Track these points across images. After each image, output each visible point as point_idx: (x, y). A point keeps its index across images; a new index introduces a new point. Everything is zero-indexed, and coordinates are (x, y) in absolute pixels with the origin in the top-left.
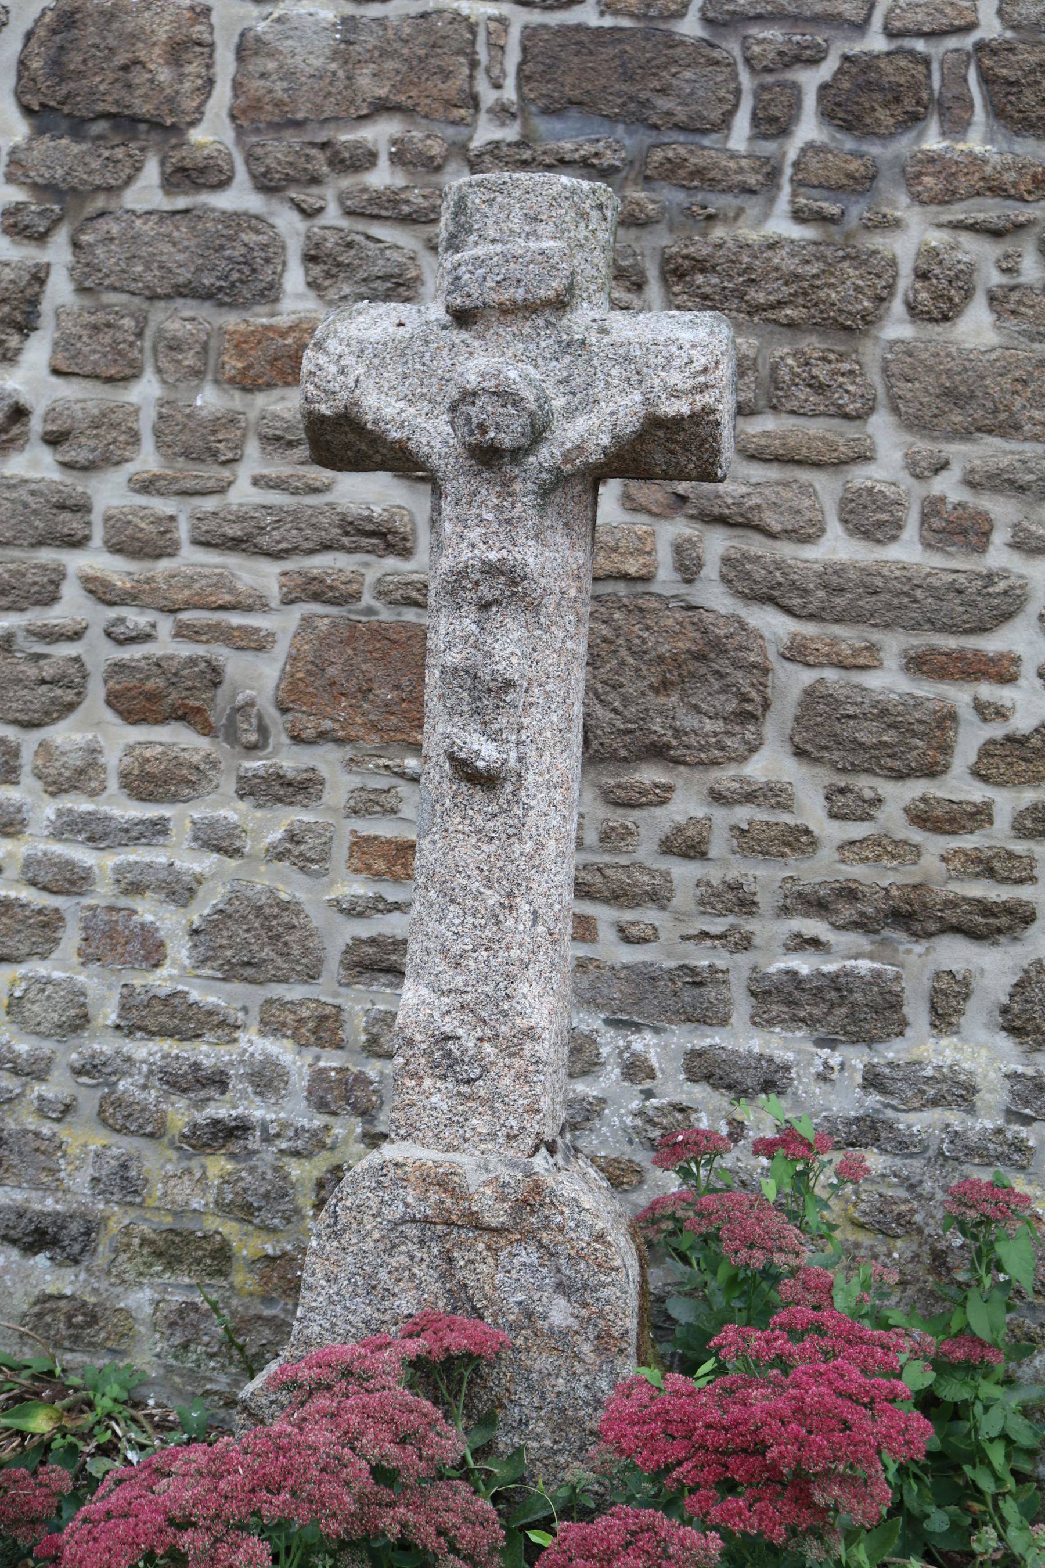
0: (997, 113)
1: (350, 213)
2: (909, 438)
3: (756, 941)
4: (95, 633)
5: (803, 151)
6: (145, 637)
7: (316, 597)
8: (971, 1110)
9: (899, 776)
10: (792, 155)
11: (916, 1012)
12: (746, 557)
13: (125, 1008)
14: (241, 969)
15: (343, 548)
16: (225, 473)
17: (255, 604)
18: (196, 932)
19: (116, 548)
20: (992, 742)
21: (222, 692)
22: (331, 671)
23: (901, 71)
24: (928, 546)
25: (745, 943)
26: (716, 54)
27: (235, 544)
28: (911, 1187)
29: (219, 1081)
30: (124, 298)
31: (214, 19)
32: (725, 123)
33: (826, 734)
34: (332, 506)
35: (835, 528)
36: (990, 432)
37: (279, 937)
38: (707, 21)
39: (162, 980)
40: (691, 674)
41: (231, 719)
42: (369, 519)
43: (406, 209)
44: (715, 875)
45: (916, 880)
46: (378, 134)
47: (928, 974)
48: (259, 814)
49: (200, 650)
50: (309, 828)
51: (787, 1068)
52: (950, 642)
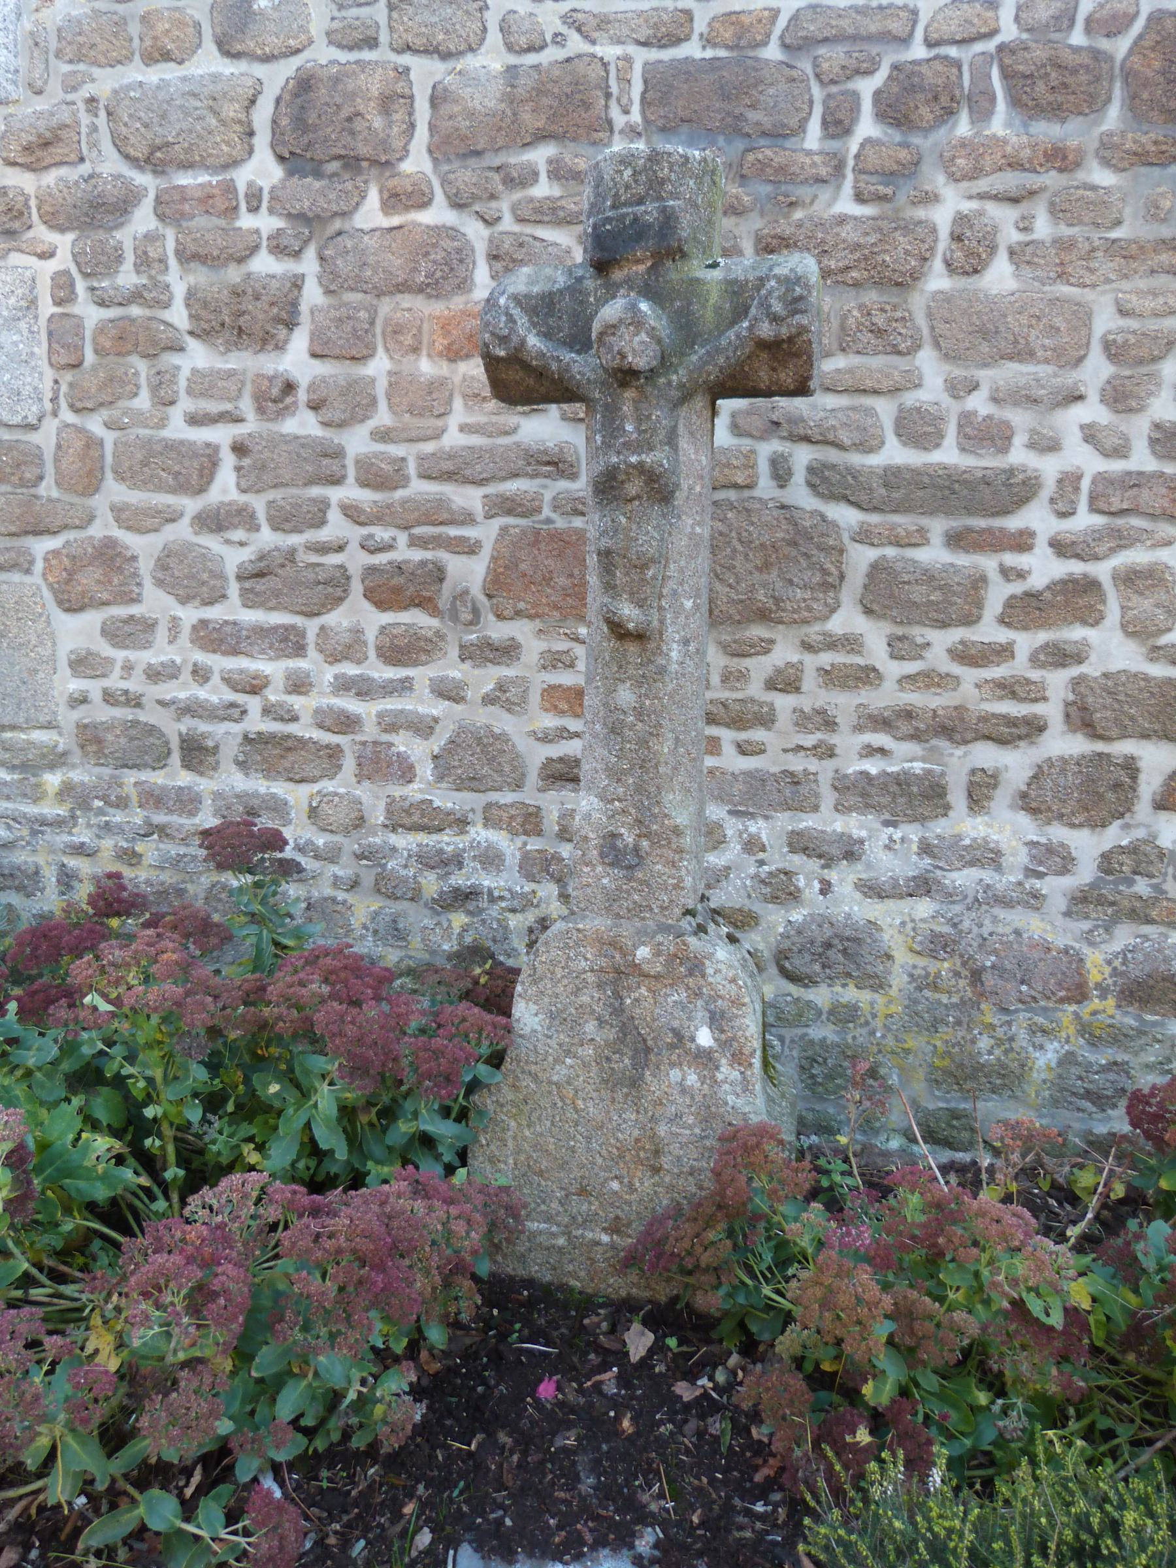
0: (1015, 102)
1: (521, 220)
2: (947, 367)
3: (837, 751)
4: (354, 546)
5: (862, 145)
6: (389, 547)
7: (510, 512)
8: (999, 868)
9: (944, 625)
10: (854, 148)
11: (957, 798)
12: (825, 466)
13: (389, 812)
14: (471, 783)
15: (527, 475)
16: (440, 423)
17: (468, 519)
18: (435, 757)
19: (364, 484)
20: (1013, 597)
21: (446, 587)
22: (523, 566)
23: (937, 74)
24: (963, 450)
25: (831, 753)
26: (794, 73)
27: (449, 476)
28: (955, 925)
29: (457, 861)
30: (360, 296)
31: (413, 76)
32: (802, 127)
33: (885, 593)
34: (518, 445)
35: (891, 440)
36: (1011, 359)
37: (494, 758)
38: (785, 46)
39: (414, 791)
40: (786, 557)
41: (453, 603)
42: (545, 452)
43: (561, 214)
44: (806, 703)
45: (957, 703)
46: (540, 156)
47: (965, 771)
48: (476, 672)
49: (429, 555)
50: (514, 681)
51: (861, 842)
52: (981, 523)
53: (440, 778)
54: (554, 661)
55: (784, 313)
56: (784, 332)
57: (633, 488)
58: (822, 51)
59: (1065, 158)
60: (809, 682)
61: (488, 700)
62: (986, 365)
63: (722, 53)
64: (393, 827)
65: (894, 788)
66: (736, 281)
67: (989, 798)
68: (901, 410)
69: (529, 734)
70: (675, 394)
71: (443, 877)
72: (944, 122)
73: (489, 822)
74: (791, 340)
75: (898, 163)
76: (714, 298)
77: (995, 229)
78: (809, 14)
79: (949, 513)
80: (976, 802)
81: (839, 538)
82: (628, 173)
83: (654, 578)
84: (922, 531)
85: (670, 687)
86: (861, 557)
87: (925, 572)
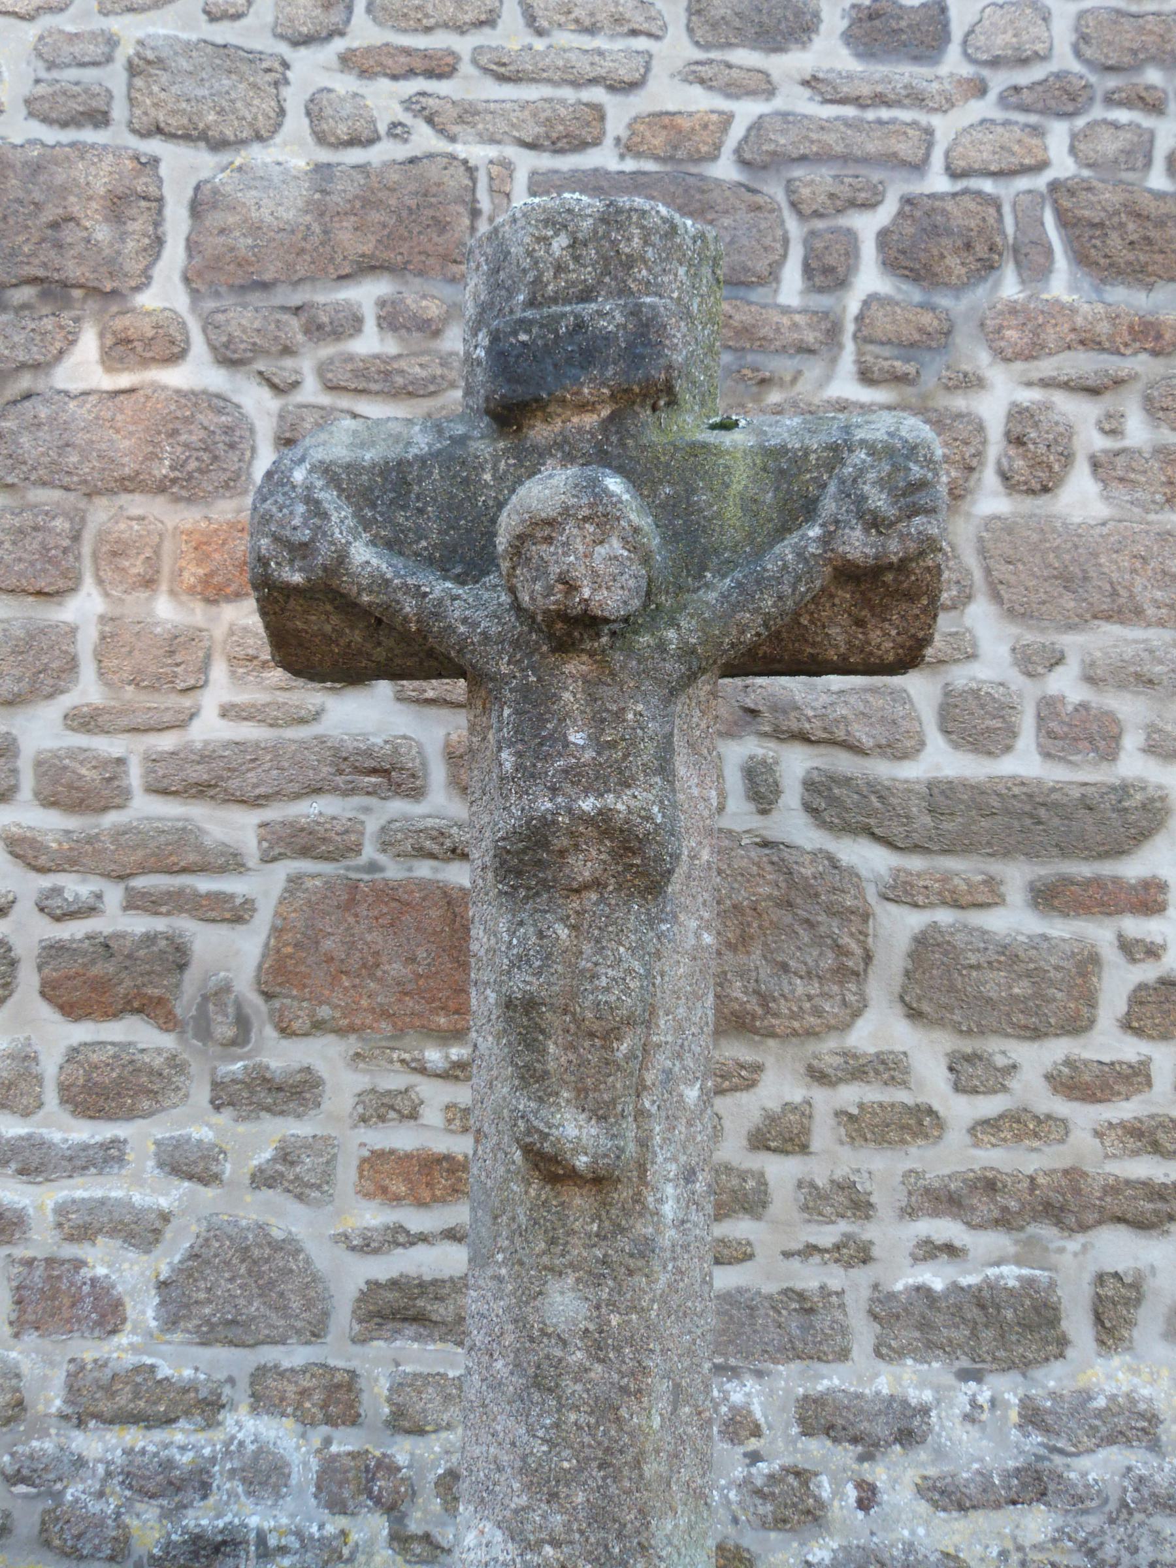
0: (1081, 258)
1: (332, 388)
2: (1014, 630)
3: (876, 1252)
4: (25, 909)
5: (866, 303)
6: (89, 910)
7: (305, 852)
8: (1155, 1446)
9: (1036, 1034)
10: (853, 307)
11: (1078, 1325)
12: (834, 779)
13: (73, 1390)
14: (228, 1331)
15: (335, 790)
16: (187, 702)
17: (232, 863)
18: (163, 1285)
19: (49, 802)
20: (1142, 987)
22: (328, 944)
23: (967, 213)
24: (1047, 755)
25: (863, 1255)
26: (759, 199)
27: (200, 791)
28: (1091, 1553)
29: (199, 1482)
30: (56, 495)
31: (163, 170)
32: (773, 275)
33: (940, 985)
34: (321, 740)
35: (936, 741)
36: (1108, 618)
37: (272, 1283)
38: (744, 163)
39: (120, 1350)
40: (774, 925)
41: (202, 1008)
42: (368, 753)
43: (399, 380)
44: (819, 1170)
45: (1067, 1163)
46: (366, 294)
47: (1088, 1277)
48: (241, 1128)
49: (159, 924)
51: (925, 1411)
52: (1084, 870)
53: (171, 1322)
54: (383, 1108)
55: (892, 512)
56: (894, 548)
57: (583, 867)
58: (798, 172)
59: (1159, 337)
60: (823, 1135)
61: (262, 1179)
62: (1070, 627)
63: (650, 166)
64: (79, 1417)
65: (973, 1313)
66: (782, 450)
67: (1130, 1323)
68: (947, 694)
69: (337, 1239)
70: (673, 668)
71: (171, 1515)
72: (983, 279)
73: (261, 1402)
74: (902, 567)
75: (921, 330)
76: (740, 480)
77: (1069, 432)
78: (778, 124)
79: (1032, 854)
80: (1109, 1331)
81: (861, 894)
82: (560, 243)
83: (628, 1058)
84: (991, 882)
85: (663, 1280)
86: (898, 926)
87: (1003, 949)
